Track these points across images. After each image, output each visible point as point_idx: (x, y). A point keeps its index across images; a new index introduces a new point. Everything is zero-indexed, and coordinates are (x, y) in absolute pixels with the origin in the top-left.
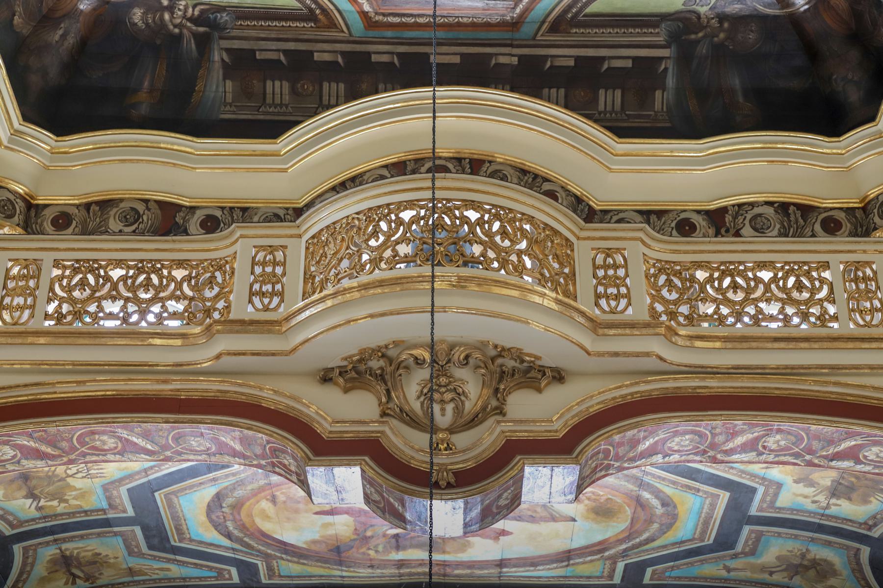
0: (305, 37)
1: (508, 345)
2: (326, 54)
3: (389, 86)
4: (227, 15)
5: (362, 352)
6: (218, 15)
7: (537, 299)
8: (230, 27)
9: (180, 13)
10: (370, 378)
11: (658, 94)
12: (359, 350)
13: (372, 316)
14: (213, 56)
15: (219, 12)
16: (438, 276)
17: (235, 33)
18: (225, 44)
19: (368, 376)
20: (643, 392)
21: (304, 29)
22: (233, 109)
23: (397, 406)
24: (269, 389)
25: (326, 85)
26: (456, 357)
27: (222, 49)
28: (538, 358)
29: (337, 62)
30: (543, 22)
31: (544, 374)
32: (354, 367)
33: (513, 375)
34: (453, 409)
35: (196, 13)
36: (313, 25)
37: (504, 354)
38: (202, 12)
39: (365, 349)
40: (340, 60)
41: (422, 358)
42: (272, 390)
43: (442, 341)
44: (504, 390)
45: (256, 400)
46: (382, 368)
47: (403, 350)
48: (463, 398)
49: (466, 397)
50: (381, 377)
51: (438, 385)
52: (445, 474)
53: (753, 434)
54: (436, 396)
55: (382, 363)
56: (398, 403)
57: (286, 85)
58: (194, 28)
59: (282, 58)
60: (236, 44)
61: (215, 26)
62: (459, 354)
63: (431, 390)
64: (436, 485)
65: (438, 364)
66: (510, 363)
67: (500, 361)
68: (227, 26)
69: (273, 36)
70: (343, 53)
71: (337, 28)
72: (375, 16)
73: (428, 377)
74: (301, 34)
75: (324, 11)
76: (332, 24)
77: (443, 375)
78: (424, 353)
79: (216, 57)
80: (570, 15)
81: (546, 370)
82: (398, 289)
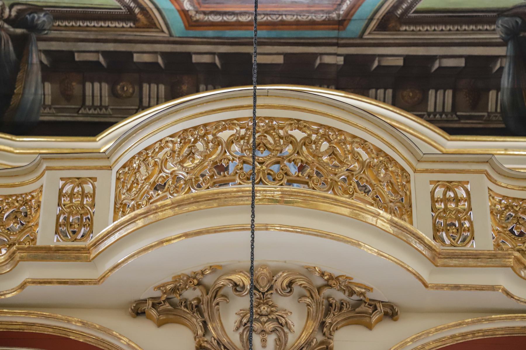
0: (124, 38)
1: (336, 273)
3: (210, 86)
4: (44, 15)
6: (36, 15)
8: (48, 28)
11: (492, 94)
14: (32, 59)
15: (36, 13)
16: (260, 191)
17: (54, 34)
24: (78, 322)
25: (146, 87)
29: (157, 64)
30: (371, 19)
32: (167, 299)
35: (13, 13)
36: (132, 25)
37: (331, 282)
38: (19, 12)
40: (160, 61)
42: (81, 322)
44: (331, 324)
45: (64, 332)
48: (286, 330)
49: (290, 329)
51: (258, 314)
55: (198, 292)
57: (105, 87)
58: (12, 29)
59: (101, 59)
60: (55, 46)
61: (32, 27)
62: (282, 280)
67: (326, 292)
68: (45, 27)
70: (163, 54)
71: (157, 28)
75: (144, 10)
77: (264, 304)
79: (35, 60)
80: (399, 12)
81: (378, 305)
82: (215, 205)
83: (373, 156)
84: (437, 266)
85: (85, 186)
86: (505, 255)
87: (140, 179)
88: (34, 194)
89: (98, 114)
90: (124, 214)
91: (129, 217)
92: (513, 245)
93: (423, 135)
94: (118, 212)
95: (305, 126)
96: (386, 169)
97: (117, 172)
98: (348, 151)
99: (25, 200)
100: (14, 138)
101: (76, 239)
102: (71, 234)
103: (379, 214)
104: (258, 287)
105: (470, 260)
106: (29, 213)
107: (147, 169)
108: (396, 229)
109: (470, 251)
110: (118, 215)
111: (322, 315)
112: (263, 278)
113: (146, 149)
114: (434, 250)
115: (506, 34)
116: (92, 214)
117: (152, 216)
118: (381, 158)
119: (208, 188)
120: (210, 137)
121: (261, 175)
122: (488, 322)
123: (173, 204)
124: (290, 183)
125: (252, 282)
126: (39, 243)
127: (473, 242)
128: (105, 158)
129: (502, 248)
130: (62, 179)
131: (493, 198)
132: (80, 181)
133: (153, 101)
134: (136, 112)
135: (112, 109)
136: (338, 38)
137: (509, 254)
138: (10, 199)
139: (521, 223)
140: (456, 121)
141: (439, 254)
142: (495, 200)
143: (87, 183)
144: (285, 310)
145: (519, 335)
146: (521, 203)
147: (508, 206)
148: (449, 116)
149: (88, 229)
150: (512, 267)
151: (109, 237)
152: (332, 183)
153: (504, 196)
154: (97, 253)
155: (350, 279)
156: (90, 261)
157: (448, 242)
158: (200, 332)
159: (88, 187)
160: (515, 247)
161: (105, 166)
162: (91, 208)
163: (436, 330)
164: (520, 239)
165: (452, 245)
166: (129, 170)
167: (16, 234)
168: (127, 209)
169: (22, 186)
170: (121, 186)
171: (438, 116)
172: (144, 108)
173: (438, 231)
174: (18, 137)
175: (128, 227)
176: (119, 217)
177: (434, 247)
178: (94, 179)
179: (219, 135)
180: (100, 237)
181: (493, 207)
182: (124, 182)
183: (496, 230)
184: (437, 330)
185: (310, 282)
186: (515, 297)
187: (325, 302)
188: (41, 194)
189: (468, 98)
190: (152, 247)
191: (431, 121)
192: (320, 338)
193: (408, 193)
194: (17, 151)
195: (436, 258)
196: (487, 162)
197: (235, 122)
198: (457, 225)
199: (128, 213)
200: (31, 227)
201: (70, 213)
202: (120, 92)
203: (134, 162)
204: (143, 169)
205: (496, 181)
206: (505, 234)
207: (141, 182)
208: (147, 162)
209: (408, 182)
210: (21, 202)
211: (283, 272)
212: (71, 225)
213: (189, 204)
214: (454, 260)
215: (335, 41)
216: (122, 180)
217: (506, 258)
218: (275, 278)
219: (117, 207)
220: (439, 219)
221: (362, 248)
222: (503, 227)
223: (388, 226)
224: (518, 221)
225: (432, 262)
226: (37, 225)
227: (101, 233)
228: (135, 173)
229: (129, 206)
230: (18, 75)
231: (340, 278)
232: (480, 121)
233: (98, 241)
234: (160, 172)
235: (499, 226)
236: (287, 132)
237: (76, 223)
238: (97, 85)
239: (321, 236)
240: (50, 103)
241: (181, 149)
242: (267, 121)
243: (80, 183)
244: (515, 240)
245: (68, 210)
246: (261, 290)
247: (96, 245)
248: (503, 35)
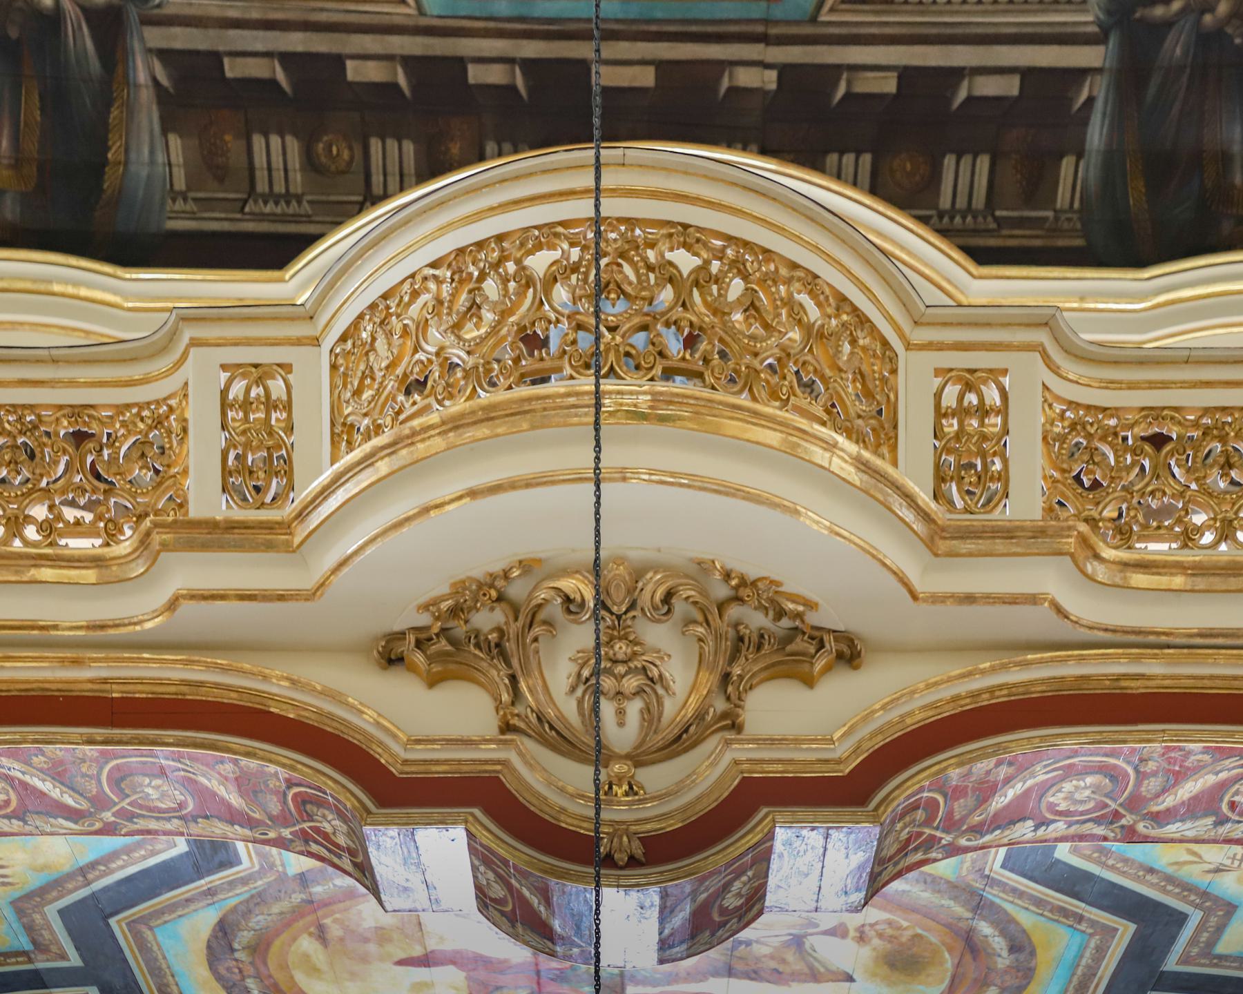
5: (459, 587)
7: (819, 455)
10: (477, 652)
12: (453, 585)
13: (473, 494)
16: (610, 393)
19: (472, 647)
20: (1015, 685)
23: (532, 711)
26: (646, 595)
28: (811, 605)
31: (821, 645)
32: (444, 630)
33: (759, 647)
34: (641, 711)
39: (463, 582)
41: (578, 599)
43: (622, 558)
46: (500, 631)
47: (543, 580)
50: (498, 650)
52: (625, 839)
53: (1217, 774)
54: (607, 683)
56: (533, 704)
63: (596, 673)
64: (609, 861)
65: (612, 613)
66: (756, 620)
73: (591, 643)
78: (581, 587)
82: (525, 426)
83: (829, 311)
84: (936, 555)
85: (270, 383)
86: (1062, 529)
87: (376, 367)
88: (173, 402)
89: (284, 215)
90: (350, 446)
91: (362, 455)
92: (1078, 510)
93: (926, 264)
94: (339, 442)
95: (698, 241)
96: (853, 342)
97: (331, 351)
98: (782, 300)
99: (156, 416)
100: (120, 271)
101: (263, 504)
102: (253, 493)
103: (835, 445)
104: (609, 603)
105: (997, 541)
106: (167, 446)
107: (389, 344)
108: (865, 477)
109: (1000, 523)
110: (339, 449)
111: (725, 658)
112: (618, 586)
113: (385, 297)
114: (933, 521)
115: (1109, 13)
116: (289, 447)
117: (404, 452)
118: (845, 317)
119: (510, 388)
120: (511, 267)
121: (612, 357)
122: (1018, 668)
123: (443, 423)
124: (668, 374)
125: (598, 593)
126: (195, 511)
127: (1005, 505)
128: (304, 318)
129: (1057, 514)
130: (224, 367)
131: (1050, 406)
132: (260, 373)
133: (393, 182)
134: (360, 208)
135: (310, 202)
136: (766, 22)
137: (1070, 528)
138: (128, 414)
139: (1096, 460)
140: (993, 230)
141: (943, 530)
142: (1054, 412)
143: (274, 378)
144: (658, 651)
145: (1071, 692)
146: (1100, 416)
147: (1076, 423)
148: (980, 219)
149: (285, 480)
150: (1072, 555)
151: (325, 499)
152: (748, 376)
153: (1070, 403)
154: (306, 533)
155: (778, 584)
156: (294, 551)
157: (959, 504)
158: (505, 697)
159: (277, 387)
160: (1080, 513)
161: (307, 338)
162: (286, 434)
163: (927, 685)
164: (1091, 496)
165: (967, 511)
166: (354, 345)
167: (148, 492)
168: (356, 437)
169: (147, 383)
170: (340, 383)
171: (958, 220)
172: (376, 200)
173: (943, 480)
174: (128, 270)
175: (359, 477)
176: (341, 454)
177: (933, 516)
178: (287, 367)
179: (529, 261)
180: (309, 499)
181: (1048, 427)
182: (345, 375)
183: (1051, 477)
184: (928, 687)
185: (703, 592)
186: (1072, 617)
187: (731, 633)
188: (187, 403)
189: (1019, 176)
190: (408, 519)
191: (943, 233)
192: (720, 705)
193: (892, 396)
194: (130, 305)
195: (936, 538)
196: (1046, 324)
197: (560, 229)
198: (979, 468)
199: (359, 446)
200: (175, 476)
201: (248, 446)
202: (323, 159)
203: (362, 328)
204: (381, 344)
205: (1058, 368)
206: (1064, 485)
207: (379, 375)
208: (389, 327)
209: (894, 371)
210: (149, 422)
211: (656, 573)
212: (251, 472)
213: (475, 423)
214: (968, 541)
215: (760, 29)
216: (342, 369)
217: (1063, 537)
218: (640, 585)
219: (337, 431)
220: (947, 455)
221: (802, 519)
222: (1063, 471)
223: (852, 470)
224: (1092, 457)
225: (927, 546)
226: (185, 472)
227: (310, 489)
228: (367, 354)
229: (359, 429)
230: (112, 116)
231: (760, 584)
232: (1039, 232)
233: (306, 507)
234: (415, 351)
235: (1056, 468)
236: (663, 256)
237: (260, 469)
239: (727, 494)
240: (183, 188)
241: (454, 296)
242: (623, 228)
243: (260, 378)
244: (1083, 497)
245: (243, 439)
246: (615, 609)
247: (302, 515)
248: (1101, 16)
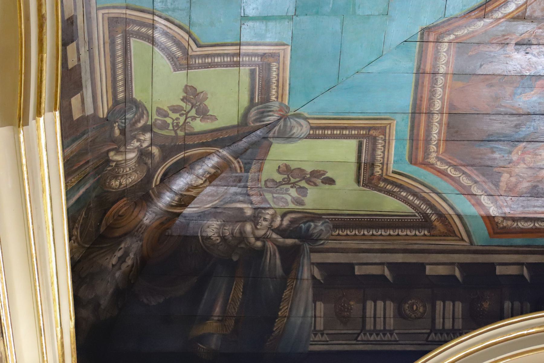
0: (416, 247)
2: (440, 267)
6: (312, 224)
9: (265, 223)
15: (312, 221)
17: (331, 244)
18: (317, 258)
21: (415, 238)
22: (326, 337)
25: (439, 305)
27: (313, 264)
29: (454, 277)
35: (285, 222)
36: (426, 233)
38: (292, 221)
40: (457, 273)
57: (391, 306)
58: (281, 240)
59: (387, 273)
60: (332, 258)
69: (377, 247)
70: (462, 266)
71: (456, 236)
72: (502, 222)
74: (411, 244)
76: (451, 232)
238: (380, 304)
